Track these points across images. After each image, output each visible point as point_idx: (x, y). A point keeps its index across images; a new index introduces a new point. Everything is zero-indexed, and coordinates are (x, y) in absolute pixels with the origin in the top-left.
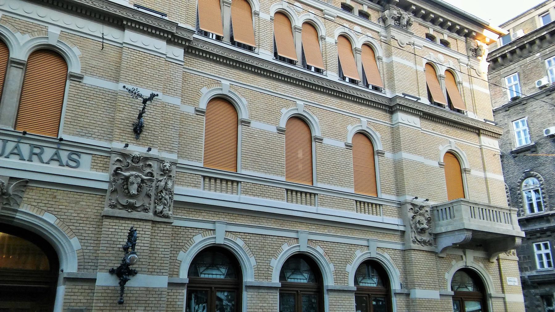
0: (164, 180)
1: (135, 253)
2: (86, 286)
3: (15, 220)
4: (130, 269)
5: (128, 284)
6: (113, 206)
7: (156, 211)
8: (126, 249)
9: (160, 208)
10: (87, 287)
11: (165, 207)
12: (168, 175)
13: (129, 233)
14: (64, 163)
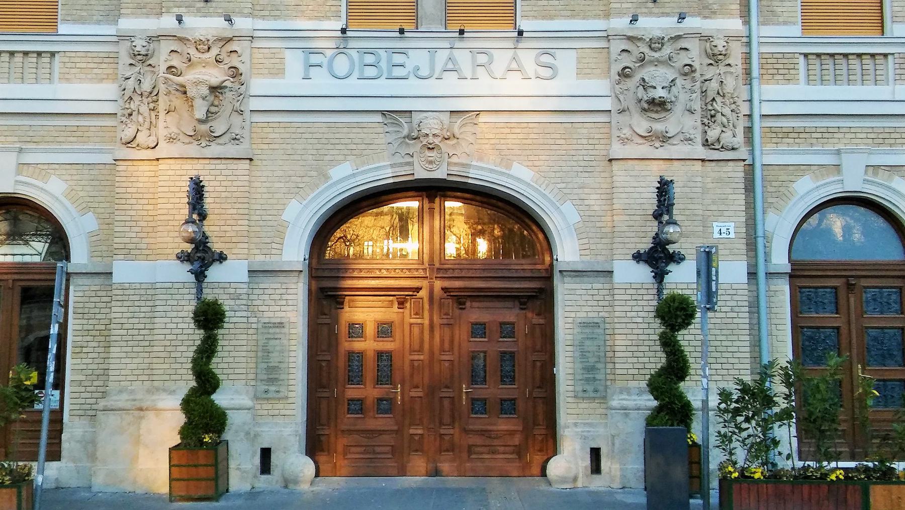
0: (715, 77)
1: (675, 223)
2: (598, 284)
3: (470, 181)
4: (671, 251)
5: (667, 279)
6: (624, 141)
7: (707, 140)
8: (657, 216)
9: (713, 134)
10: (600, 286)
11: (724, 129)
12: (723, 64)
13: (657, 188)
14: (531, 74)
